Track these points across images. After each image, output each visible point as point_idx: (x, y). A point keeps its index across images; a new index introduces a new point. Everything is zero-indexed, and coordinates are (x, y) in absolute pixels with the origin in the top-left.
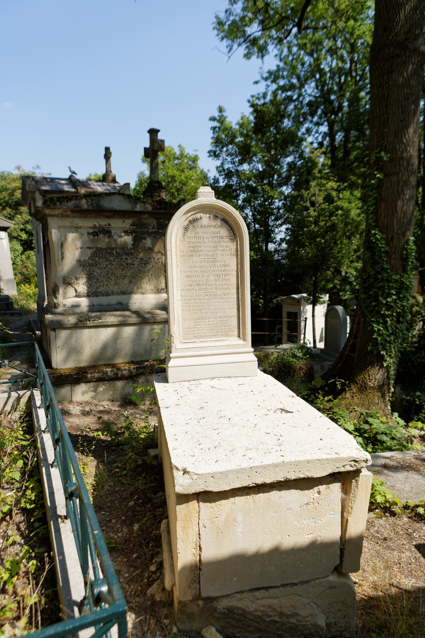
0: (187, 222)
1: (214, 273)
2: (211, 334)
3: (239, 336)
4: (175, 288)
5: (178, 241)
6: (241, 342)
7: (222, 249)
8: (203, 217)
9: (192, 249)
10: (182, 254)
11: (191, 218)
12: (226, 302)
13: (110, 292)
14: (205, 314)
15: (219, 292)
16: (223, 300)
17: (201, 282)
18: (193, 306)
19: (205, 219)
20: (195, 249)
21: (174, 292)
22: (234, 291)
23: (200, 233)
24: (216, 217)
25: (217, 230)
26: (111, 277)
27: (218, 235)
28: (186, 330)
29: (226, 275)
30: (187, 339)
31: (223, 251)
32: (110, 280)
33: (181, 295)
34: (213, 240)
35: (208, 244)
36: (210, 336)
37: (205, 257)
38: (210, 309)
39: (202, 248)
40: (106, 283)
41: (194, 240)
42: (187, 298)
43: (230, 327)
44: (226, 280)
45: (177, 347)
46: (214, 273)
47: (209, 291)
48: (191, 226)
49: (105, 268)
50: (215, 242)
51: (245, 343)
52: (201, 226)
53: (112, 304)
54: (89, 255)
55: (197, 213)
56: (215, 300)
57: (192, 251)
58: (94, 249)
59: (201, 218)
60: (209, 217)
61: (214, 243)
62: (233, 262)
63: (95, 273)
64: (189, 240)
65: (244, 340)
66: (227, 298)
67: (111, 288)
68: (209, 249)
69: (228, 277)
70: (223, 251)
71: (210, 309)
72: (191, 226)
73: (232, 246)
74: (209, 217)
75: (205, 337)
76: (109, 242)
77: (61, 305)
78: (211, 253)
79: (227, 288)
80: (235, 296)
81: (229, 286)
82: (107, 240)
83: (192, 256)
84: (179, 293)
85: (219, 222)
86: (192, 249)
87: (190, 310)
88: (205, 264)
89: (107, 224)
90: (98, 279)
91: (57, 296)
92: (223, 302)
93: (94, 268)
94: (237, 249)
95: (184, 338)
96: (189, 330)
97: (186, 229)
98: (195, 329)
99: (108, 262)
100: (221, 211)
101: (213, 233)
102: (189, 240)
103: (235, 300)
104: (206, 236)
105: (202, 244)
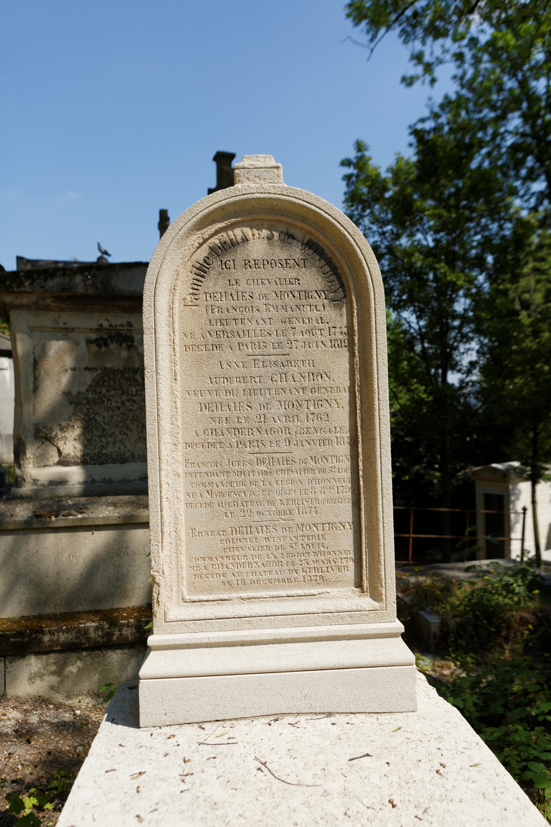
0: (203, 252)
1: (283, 397)
2: (274, 576)
3: (359, 584)
4: (166, 439)
5: (177, 305)
6: (367, 602)
7: (306, 326)
8: (250, 236)
9: (219, 327)
10: (189, 341)
11: (215, 240)
12: (318, 481)
13: (127, 454)
14: (256, 518)
15: (298, 453)
16: (310, 476)
17: (244, 424)
18: (222, 494)
19: (257, 243)
20: (228, 328)
21: (164, 452)
22: (344, 449)
23: (243, 282)
24: (288, 237)
25: (292, 274)
26: (131, 426)
27: (296, 287)
28: (201, 562)
29: (318, 403)
30: (203, 591)
31: (310, 332)
32: (129, 432)
33: (187, 461)
34: (279, 302)
35: (265, 315)
36: (271, 583)
37: (257, 351)
38: (271, 502)
39: (248, 325)
40: (120, 437)
41: (224, 303)
42: (204, 469)
43: (332, 557)
44: (318, 417)
45: (170, 617)
46: (283, 397)
47: (269, 449)
48: (216, 264)
49: (118, 408)
50: (285, 308)
51: (376, 605)
52: (247, 264)
53: (131, 478)
54: (89, 382)
55: (232, 227)
56: (285, 476)
57: (219, 333)
58: (99, 371)
59: (245, 240)
60: (270, 238)
61: (282, 312)
62: (339, 366)
63: (99, 419)
64: (211, 302)
65: (376, 596)
66: (323, 470)
67: (129, 447)
68: (267, 327)
69: (326, 408)
70: (310, 332)
71: (271, 502)
72: (216, 264)
73: (337, 319)
74: (270, 238)
75: (256, 584)
76: (129, 358)
77: (28, 480)
78: (274, 338)
79: (323, 442)
80: (347, 464)
81: (328, 435)
82: (124, 354)
83: (218, 346)
84: (179, 455)
85: (297, 252)
86: (219, 327)
87: (210, 504)
88: (255, 371)
89: (125, 323)
90: (104, 430)
91: (22, 462)
92: (310, 481)
93: (97, 408)
94: (350, 326)
95: (193, 588)
96: (208, 562)
97: (202, 270)
98: (226, 561)
99: (125, 397)
100: (304, 220)
101: (280, 281)
102: (211, 302)
103: (347, 475)
104: (258, 289)
105: (248, 315)
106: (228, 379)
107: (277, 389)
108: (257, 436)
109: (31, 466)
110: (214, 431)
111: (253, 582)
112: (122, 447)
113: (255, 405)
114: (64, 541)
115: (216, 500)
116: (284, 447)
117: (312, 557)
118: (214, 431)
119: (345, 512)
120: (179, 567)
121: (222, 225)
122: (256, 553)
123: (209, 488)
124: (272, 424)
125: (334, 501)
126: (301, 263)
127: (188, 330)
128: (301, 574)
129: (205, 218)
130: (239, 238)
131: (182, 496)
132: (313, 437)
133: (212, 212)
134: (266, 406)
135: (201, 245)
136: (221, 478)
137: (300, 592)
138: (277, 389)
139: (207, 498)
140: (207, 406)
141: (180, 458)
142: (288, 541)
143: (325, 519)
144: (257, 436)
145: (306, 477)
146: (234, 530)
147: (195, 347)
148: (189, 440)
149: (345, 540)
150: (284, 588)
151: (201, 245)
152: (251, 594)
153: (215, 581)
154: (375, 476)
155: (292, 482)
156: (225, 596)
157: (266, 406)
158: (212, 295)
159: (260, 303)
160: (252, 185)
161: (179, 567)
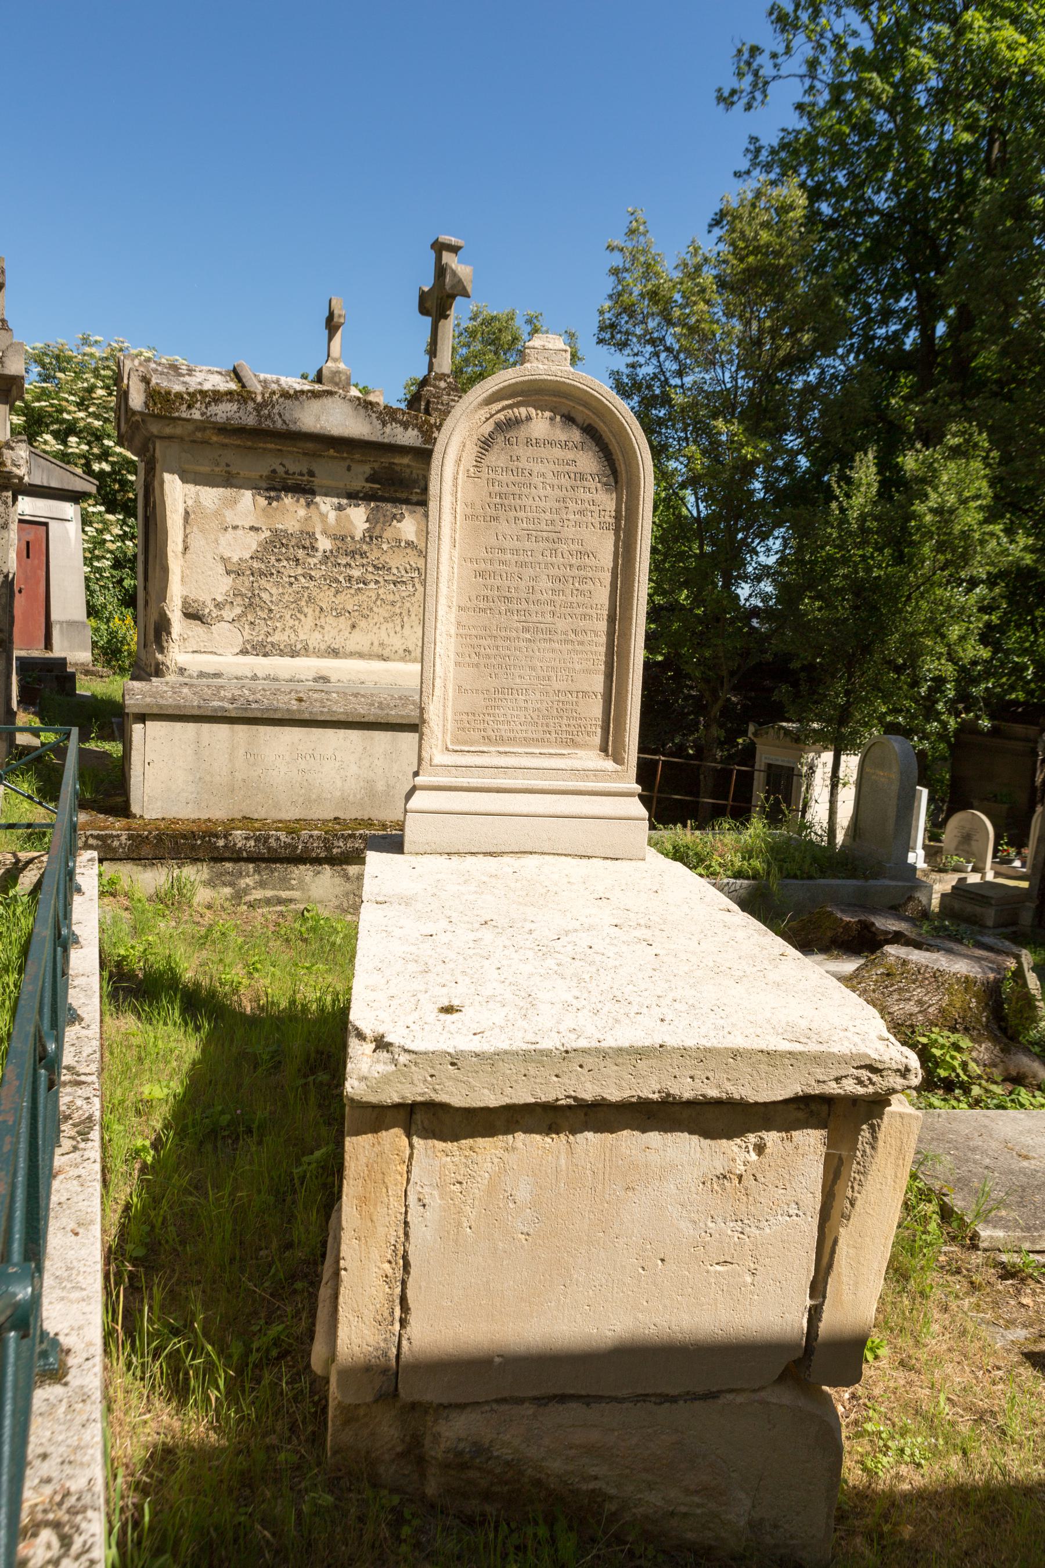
0: (489, 427)
1: (552, 572)
2: (530, 735)
3: (604, 749)
4: (443, 601)
5: (460, 476)
6: (610, 765)
7: (579, 507)
8: (534, 415)
9: (498, 500)
10: (469, 511)
11: (501, 416)
12: (577, 652)
13: (299, 646)
14: (518, 681)
15: (561, 625)
16: (570, 647)
17: (514, 594)
18: (488, 656)
19: (541, 425)
20: (506, 502)
21: (440, 613)
22: (603, 626)
23: (523, 459)
24: (569, 419)
25: (570, 455)
26: (305, 610)
27: (572, 468)
28: (465, 717)
29: (583, 580)
30: (465, 743)
31: (581, 512)
32: (302, 617)
33: (459, 623)
34: (556, 482)
35: (542, 492)
36: (527, 741)
37: (531, 526)
38: (532, 668)
39: (525, 501)
40: (291, 622)
41: (504, 478)
42: (473, 632)
43: (583, 722)
44: (582, 593)
45: (435, 761)
46: (552, 572)
47: (535, 619)
48: (500, 439)
49: (291, 584)
50: (560, 488)
51: (619, 767)
52: (528, 442)
53: (303, 678)
54: (254, 547)
55: (518, 405)
56: (547, 645)
57: (496, 507)
58: (268, 534)
59: (529, 418)
60: (551, 419)
61: (557, 491)
62: (605, 547)
63: (265, 596)
64: (492, 475)
65: (618, 760)
66: (581, 643)
67: (302, 637)
68: (542, 504)
69: (589, 586)
70: (581, 512)
71: (532, 668)
72: (500, 439)
73: (608, 502)
74: (551, 419)
75: (512, 741)
76: (308, 519)
77: (172, 667)
78: (548, 516)
79: (584, 616)
80: (603, 639)
81: (589, 611)
82: (302, 512)
83: (496, 519)
84: (452, 617)
85: (576, 435)
86: (498, 500)
87: (477, 665)
88: (528, 545)
89: (305, 471)
90: (271, 611)
91: (165, 644)
92: (569, 652)
93: (263, 582)
94: (618, 511)
95: (456, 741)
96: (471, 717)
97: (486, 444)
98: (487, 718)
99: (300, 571)
100: (586, 405)
101: (558, 462)
102: (492, 475)
103: (603, 650)
104: (537, 468)
105: (525, 491)
106: (502, 550)
107: (546, 564)
108: (524, 605)
109: (176, 650)
110: (486, 598)
111: (510, 739)
112: (292, 636)
113: (526, 577)
114: (241, 734)
115: (483, 661)
116: (548, 618)
117: (565, 721)
118: (486, 598)
119: (598, 682)
120: (445, 719)
121: (510, 402)
122: (515, 713)
123: (477, 650)
124: (539, 596)
125: (587, 671)
126: (579, 446)
127: (469, 501)
128: (554, 735)
129: (494, 394)
130: (523, 416)
131: (452, 656)
132: (576, 611)
133: (501, 389)
134: (535, 579)
135: (487, 419)
136: (489, 641)
137: (552, 751)
138: (546, 564)
139: (475, 659)
140: (481, 574)
141: (453, 620)
142: (545, 705)
143: (581, 688)
144: (524, 605)
145: (565, 647)
146: (496, 691)
147: (473, 517)
148: (462, 604)
149: (596, 710)
150: (536, 746)
151: (487, 419)
152: (507, 749)
153: (476, 735)
154: (629, 652)
155: (553, 651)
156: (485, 749)
157: (535, 579)
158: (494, 470)
159: (537, 480)
160: (541, 366)
161: (445, 719)
